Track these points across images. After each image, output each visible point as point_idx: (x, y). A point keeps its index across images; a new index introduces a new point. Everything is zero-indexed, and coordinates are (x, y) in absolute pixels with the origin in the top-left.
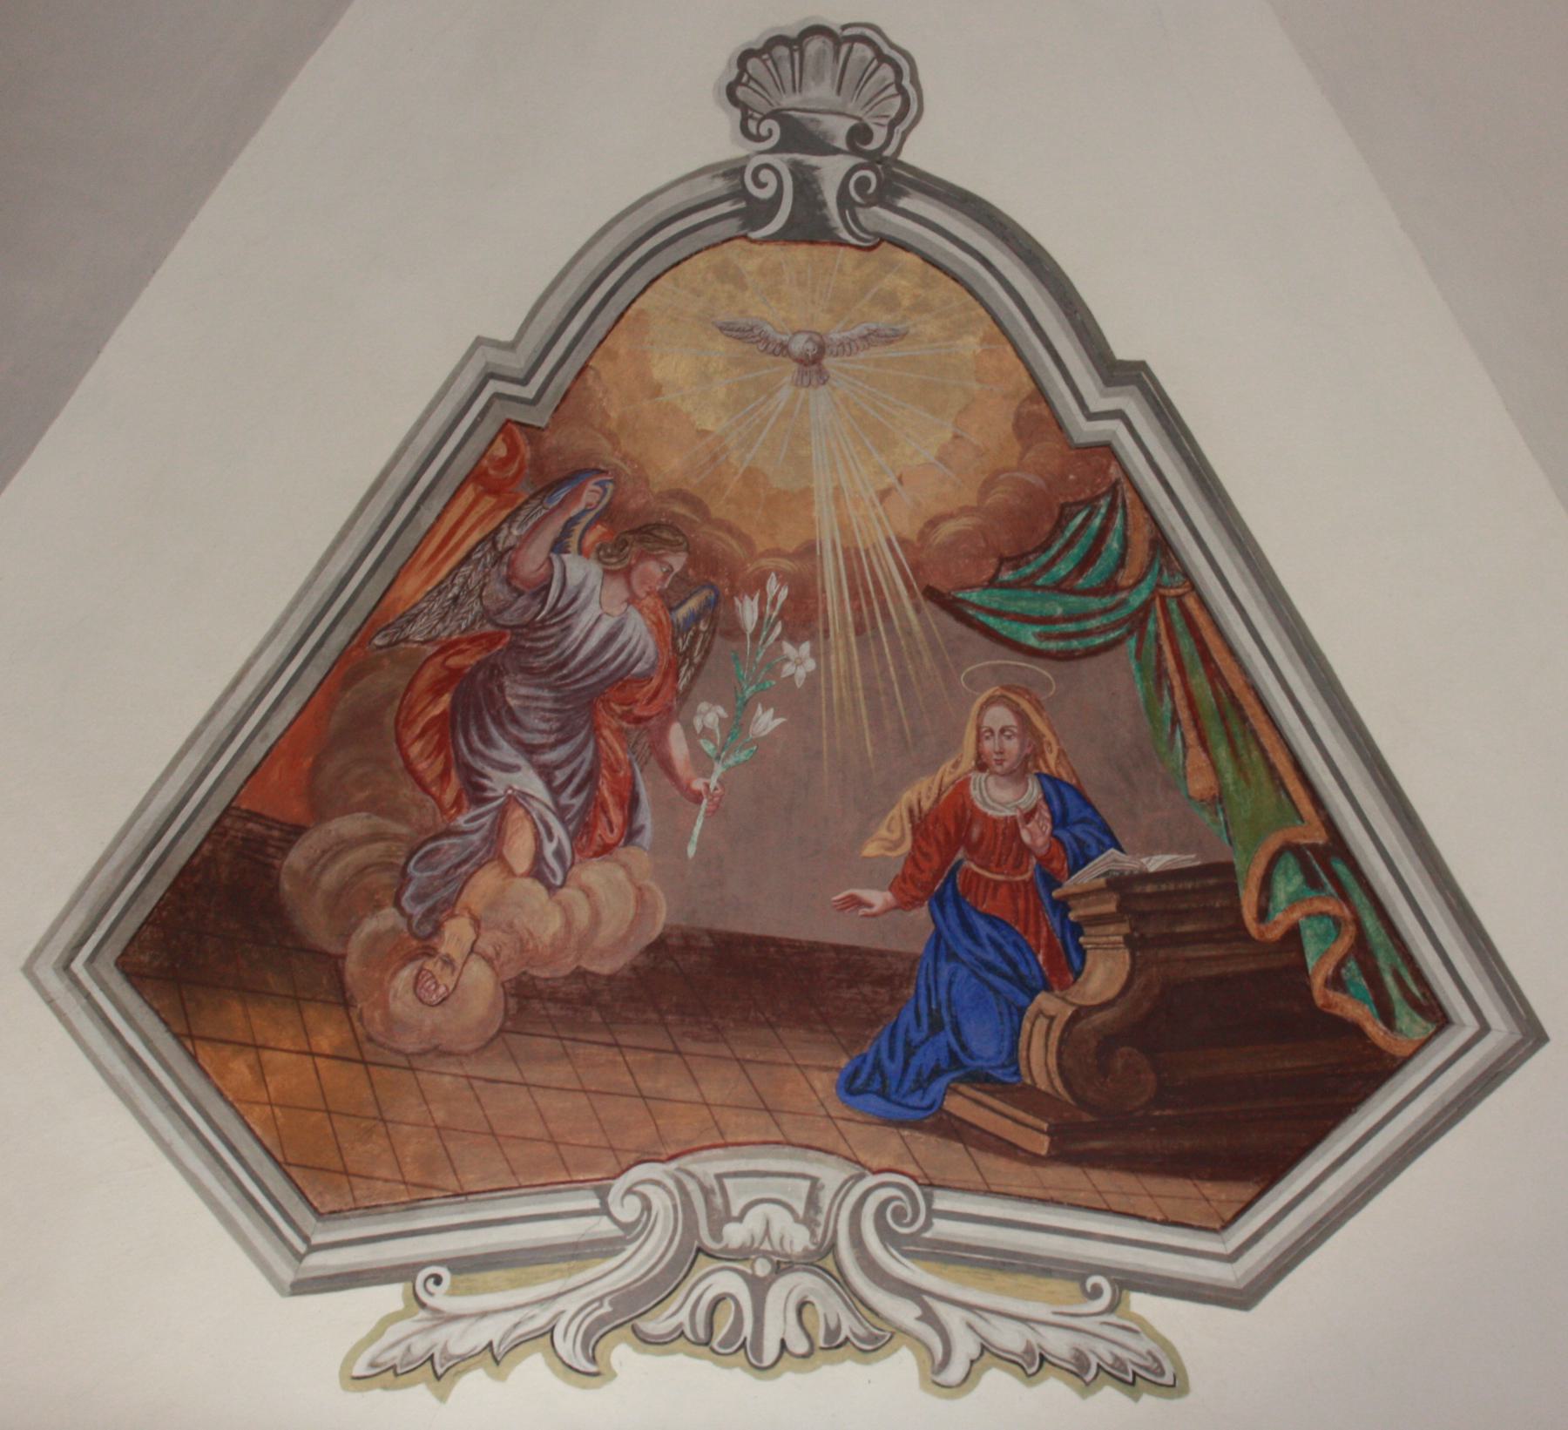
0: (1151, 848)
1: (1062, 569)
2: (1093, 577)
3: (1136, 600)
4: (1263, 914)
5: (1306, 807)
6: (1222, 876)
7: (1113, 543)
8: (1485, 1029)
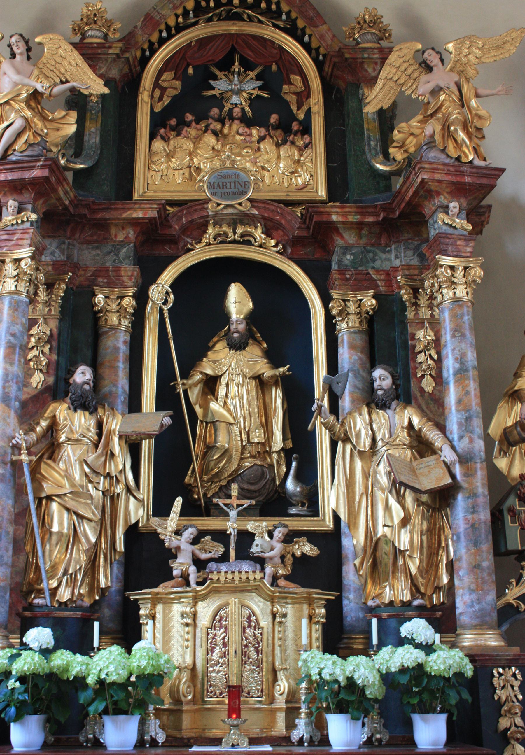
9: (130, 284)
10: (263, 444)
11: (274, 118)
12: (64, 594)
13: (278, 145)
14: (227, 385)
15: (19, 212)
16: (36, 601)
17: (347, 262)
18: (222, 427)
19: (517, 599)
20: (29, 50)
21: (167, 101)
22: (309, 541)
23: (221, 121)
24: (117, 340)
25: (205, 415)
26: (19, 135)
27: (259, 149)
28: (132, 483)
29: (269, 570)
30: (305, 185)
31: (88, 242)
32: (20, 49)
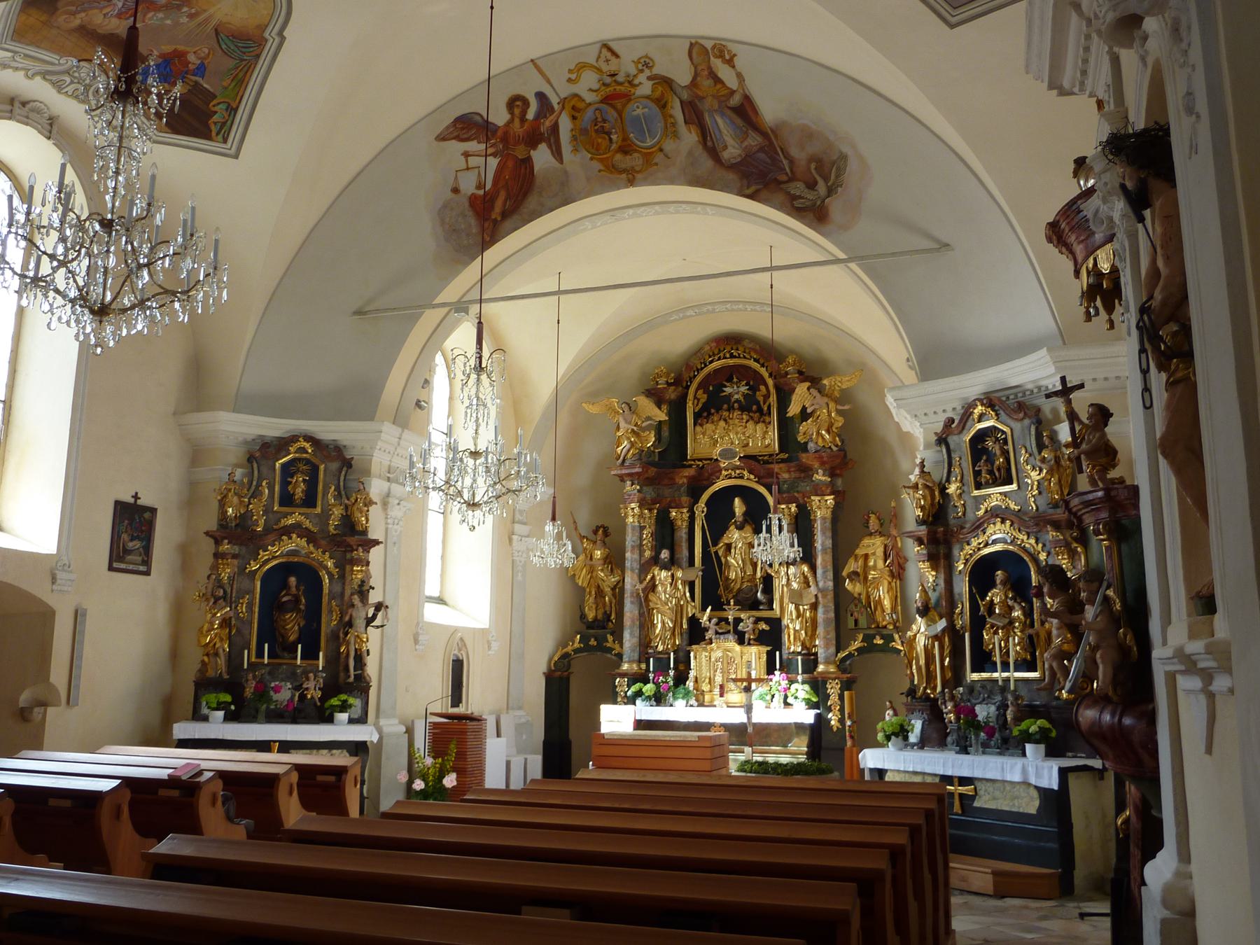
0: (207, 83)
2: (244, 50)
3: (245, 58)
4: (214, 106)
5: (238, 101)
6: (214, 96)
7: (252, 49)
8: (230, 149)
9: (686, 505)
11: (754, 407)
13: (757, 423)
18: (732, 568)
21: (700, 405)
23: (729, 410)
26: (629, 451)
27: (746, 427)
30: (769, 445)
31: (665, 485)
32: (626, 409)
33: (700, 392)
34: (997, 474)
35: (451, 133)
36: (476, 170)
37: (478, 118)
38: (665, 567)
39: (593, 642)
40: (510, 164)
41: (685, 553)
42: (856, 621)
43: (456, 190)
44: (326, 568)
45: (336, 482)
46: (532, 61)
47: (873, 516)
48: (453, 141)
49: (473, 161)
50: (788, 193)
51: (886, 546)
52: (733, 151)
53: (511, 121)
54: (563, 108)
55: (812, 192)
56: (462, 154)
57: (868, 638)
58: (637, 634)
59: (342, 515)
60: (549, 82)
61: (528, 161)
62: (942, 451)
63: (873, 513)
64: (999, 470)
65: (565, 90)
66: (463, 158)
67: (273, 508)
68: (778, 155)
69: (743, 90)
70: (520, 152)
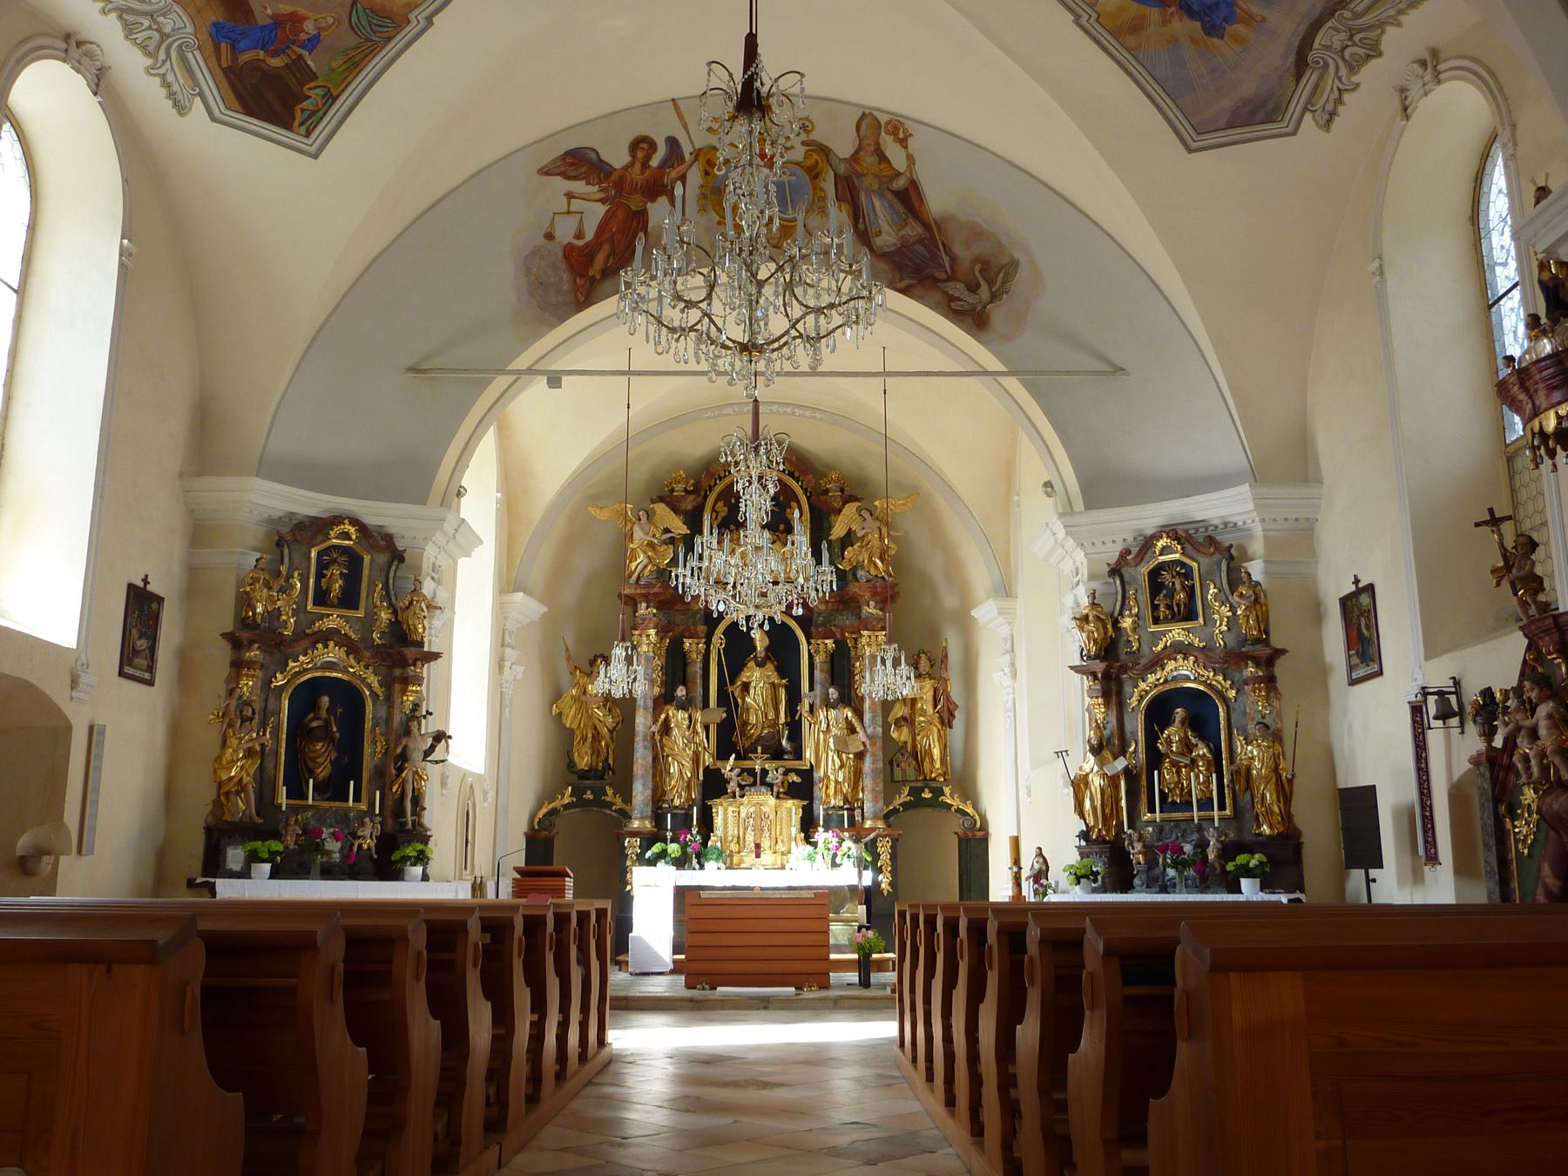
0: (314, 60)
1: (375, 21)
3: (374, 38)
4: (310, 89)
5: (341, 89)
6: (315, 77)
7: (386, 30)
8: (311, 145)
9: (703, 635)
10: (775, 720)
12: (677, 802)
14: (755, 688)
15: (647, 608)
16: (664, 805)
17: (820, 622)
18: (752, 711)
19: (900, 805)
20: (648, 516)
21: (720, 519)
22: (796, 774)
24: (696, 667)
25: (743, 704)
26: (645, 567)
28: (706, 746)
29: (775, 789)
32: (644, 518)
33: (720, 504)
34: (1176, 609)
35: (558, 167)
36: (579, 216)
37: (593, 156)
38: (683, 706)
39: (589, 796)
40: (621, 215)
41: (700, 690)
42: (904, 771)
43: (549, 236)
44: (369, 686)
45: (384, 579)
46: (673, 100)
47: (923, 656)
48: (558, 177)
49: (576, 205)
50: (946, 294)
51: (935, 690)
52: (888, 238)
53: (632, 164)
54: (696, 159)
55: (974, 296)
56: (565, 195)
57: (916, 792)
58: (650, 785)
59: (390, 620)
60: (685, 127)
61: (643, 214)
62: (1115, 583)
63: (923, 653)
64: (1179, 606)
65: (702, 139)
66: (565, 200)
67: (306, 607)
68: (939, 250)
69: (911, 175)
70: (635, 202)
